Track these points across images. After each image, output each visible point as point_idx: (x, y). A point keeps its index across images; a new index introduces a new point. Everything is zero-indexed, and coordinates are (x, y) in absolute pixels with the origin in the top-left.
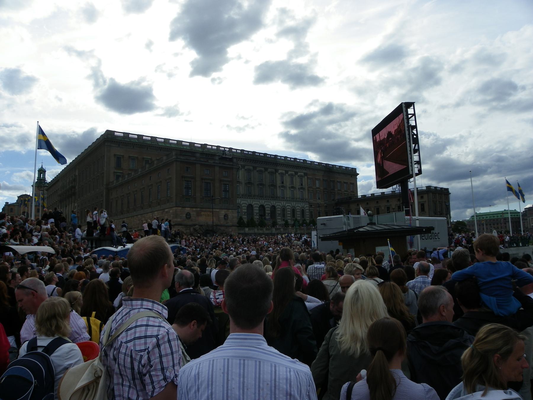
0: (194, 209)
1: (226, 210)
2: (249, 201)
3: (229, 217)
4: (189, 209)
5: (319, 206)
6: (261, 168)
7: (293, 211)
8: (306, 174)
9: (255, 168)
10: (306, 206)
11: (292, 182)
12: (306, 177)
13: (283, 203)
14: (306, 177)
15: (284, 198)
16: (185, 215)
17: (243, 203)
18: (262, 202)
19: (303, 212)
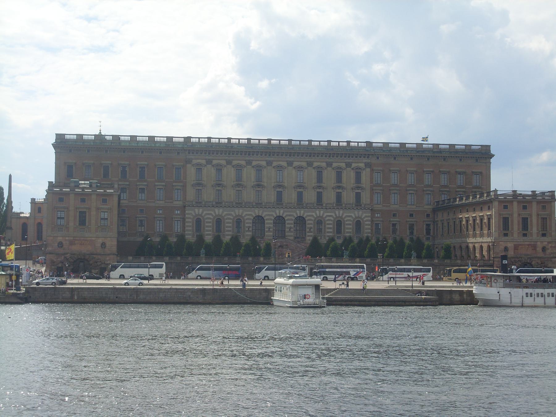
0: (67, 238)
1: (103, 239)
2: (257, 212)
3: (107, 245)
4: (61, 238)
5: (394, 215)
7: (339, 224)
8: (367, 165)
9: (269, 163)
10: (365, 216)
12: (368, 170)
13: (319, 213)
14: (368, 170)
15: (322, 205)
16: (57, 244)
17: (247, 215)
19: (358, 224)
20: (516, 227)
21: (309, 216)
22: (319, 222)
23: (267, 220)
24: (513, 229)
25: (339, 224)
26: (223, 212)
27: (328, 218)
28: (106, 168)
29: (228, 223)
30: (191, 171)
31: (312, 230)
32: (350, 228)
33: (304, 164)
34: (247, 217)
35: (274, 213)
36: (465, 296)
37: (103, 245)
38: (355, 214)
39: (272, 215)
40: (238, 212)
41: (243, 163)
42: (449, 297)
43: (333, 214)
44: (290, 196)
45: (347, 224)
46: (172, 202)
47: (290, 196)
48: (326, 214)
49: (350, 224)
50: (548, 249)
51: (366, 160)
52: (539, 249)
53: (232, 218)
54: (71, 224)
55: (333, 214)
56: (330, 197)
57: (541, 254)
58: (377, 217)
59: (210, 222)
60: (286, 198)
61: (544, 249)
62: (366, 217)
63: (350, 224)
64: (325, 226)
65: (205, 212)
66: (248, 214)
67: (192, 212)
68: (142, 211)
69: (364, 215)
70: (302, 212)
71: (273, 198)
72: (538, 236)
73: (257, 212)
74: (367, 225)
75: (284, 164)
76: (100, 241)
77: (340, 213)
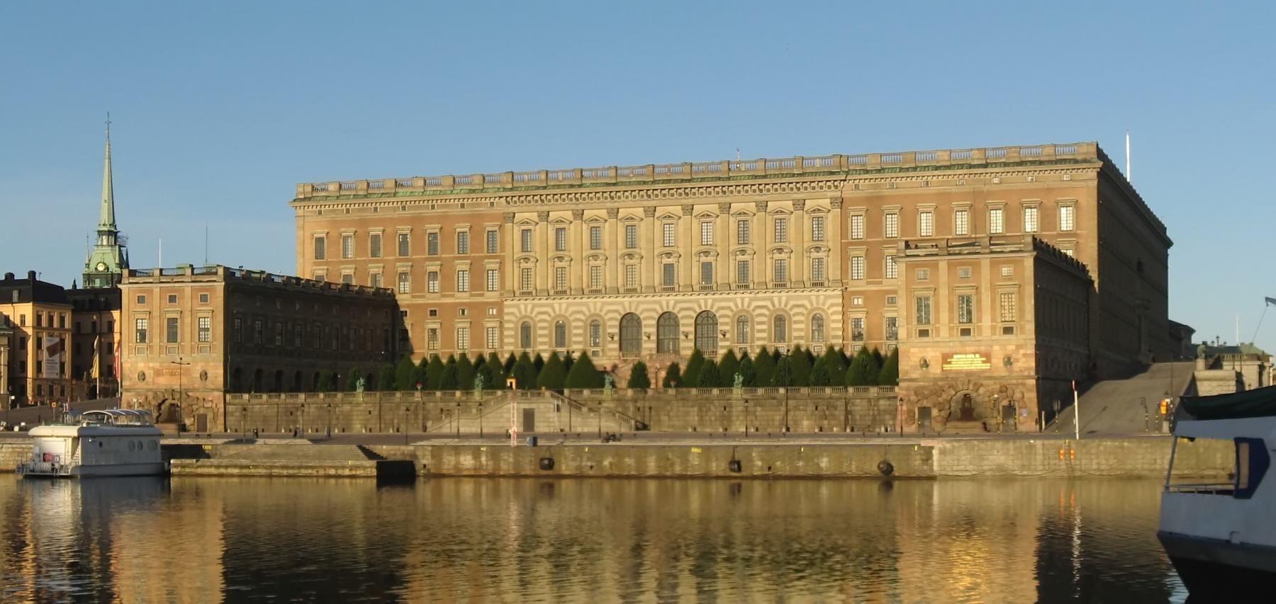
6: (671, 209)
7: (780, 322)
11: (780, 233)
15: (747, 287)
17: (609, 311)
18: (668, 302)
19: (818, 321)
20: (944, 316)
21: (723, 308)
22: (742, 321)
23: (645, 318)
24: (937, 321)
25: (780, 322)
26: (567, 309)
27: (758, 311)
28: (376, 239)
29: (576, 328)
30: (513, 234)
31: (728, 336)
32: (801, 330)
33: (714, 208)
34: (610, 315)
35: (657, 307)
36: (483, 459)
37: (204, 375)
38: (811, 302)
39: (654, 310)
40: (594, 304)
41: (603, 213)
42: (453, 463)
43: (768, 304)
44: (688, 272)
45: (796, 322)
46: (482, 295)
47: (688, 272)
48: (754, 304)
49: (801, 322)
50: (1017, 360)
51: (830, 194)
52: (998, 361)
53: (583, 317)
54: (156, 340)
55: (768, 304)
56: (762, 269)
57: (1002, 371)
58: (858, 306)
59: (544, 328)
60: (681, 276)
61: (1008, 361)
62: (833, 305)
63: (801, 322)
64: (753, 328)
65: (537, 310)
66: (611, 309)
67: (515, 310)
68: (433, 313)
69: (830, 301)
70: (710, 302)
71: (658, 278)
72: (994, 333)
73: (626, 304)
74: (834, 321)
75: (677, 210)
76: (198, 369)
77: (781, 299)
